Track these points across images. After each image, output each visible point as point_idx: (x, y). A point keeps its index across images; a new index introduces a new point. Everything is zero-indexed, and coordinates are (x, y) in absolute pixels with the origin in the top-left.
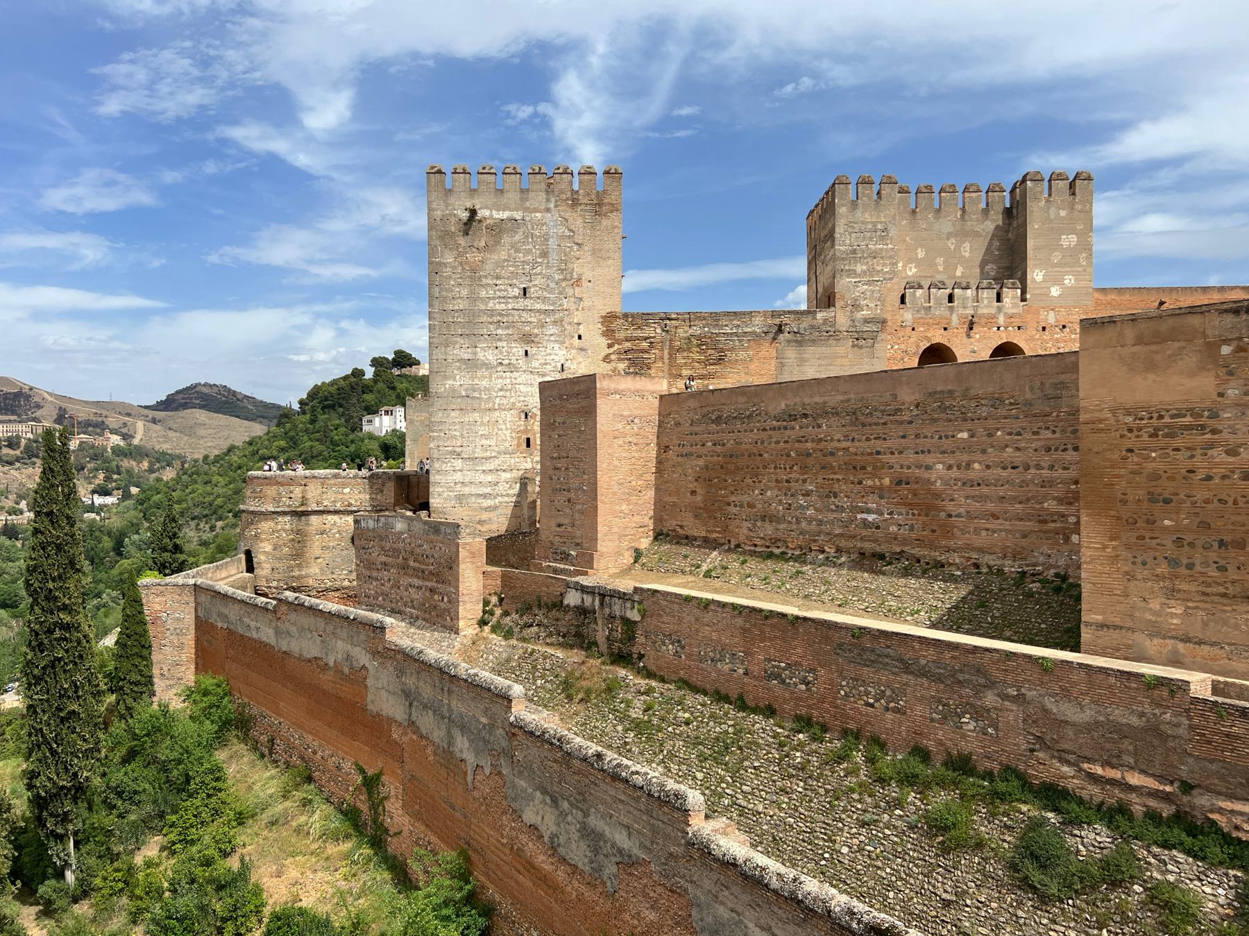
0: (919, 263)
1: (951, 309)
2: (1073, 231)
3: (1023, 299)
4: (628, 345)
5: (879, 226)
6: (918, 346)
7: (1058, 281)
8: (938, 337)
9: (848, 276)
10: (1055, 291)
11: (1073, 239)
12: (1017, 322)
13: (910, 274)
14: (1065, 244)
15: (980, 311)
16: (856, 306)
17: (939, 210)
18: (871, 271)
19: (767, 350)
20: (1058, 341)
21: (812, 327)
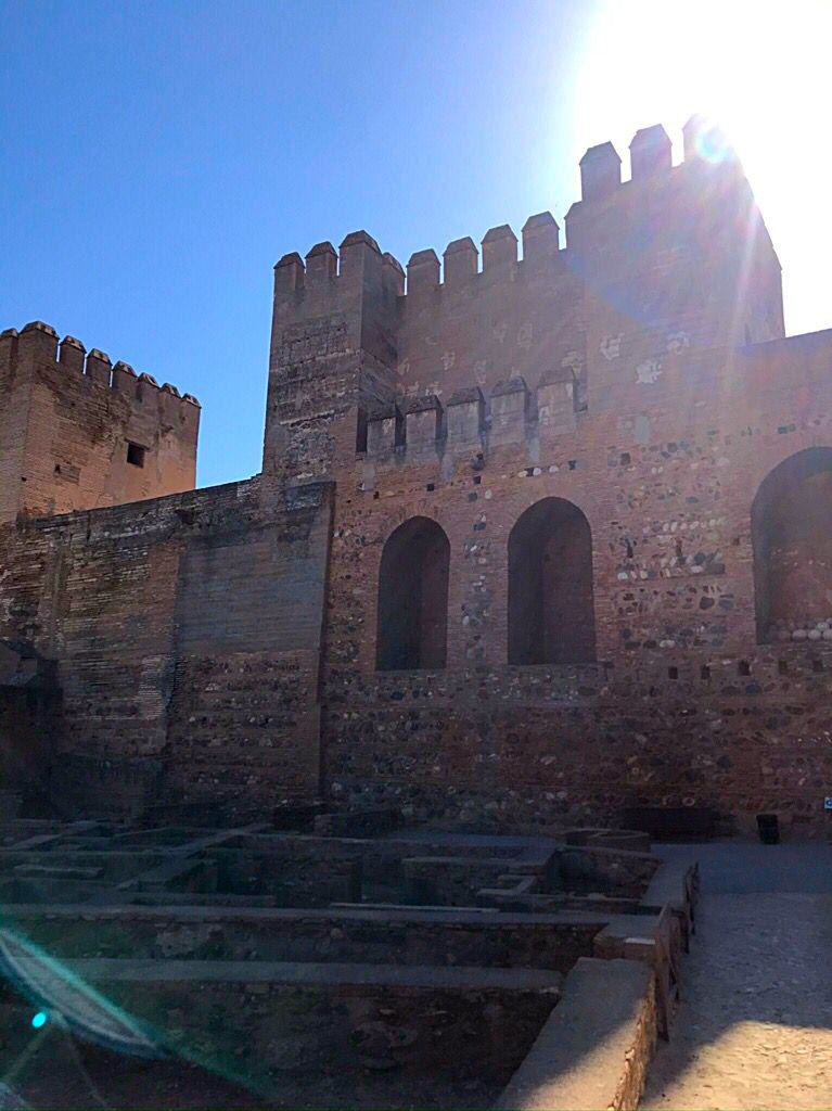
4: (17, 570)
5: (334, 323)
15: (493, 443)
18: (318, 400)
19: (170, 559)
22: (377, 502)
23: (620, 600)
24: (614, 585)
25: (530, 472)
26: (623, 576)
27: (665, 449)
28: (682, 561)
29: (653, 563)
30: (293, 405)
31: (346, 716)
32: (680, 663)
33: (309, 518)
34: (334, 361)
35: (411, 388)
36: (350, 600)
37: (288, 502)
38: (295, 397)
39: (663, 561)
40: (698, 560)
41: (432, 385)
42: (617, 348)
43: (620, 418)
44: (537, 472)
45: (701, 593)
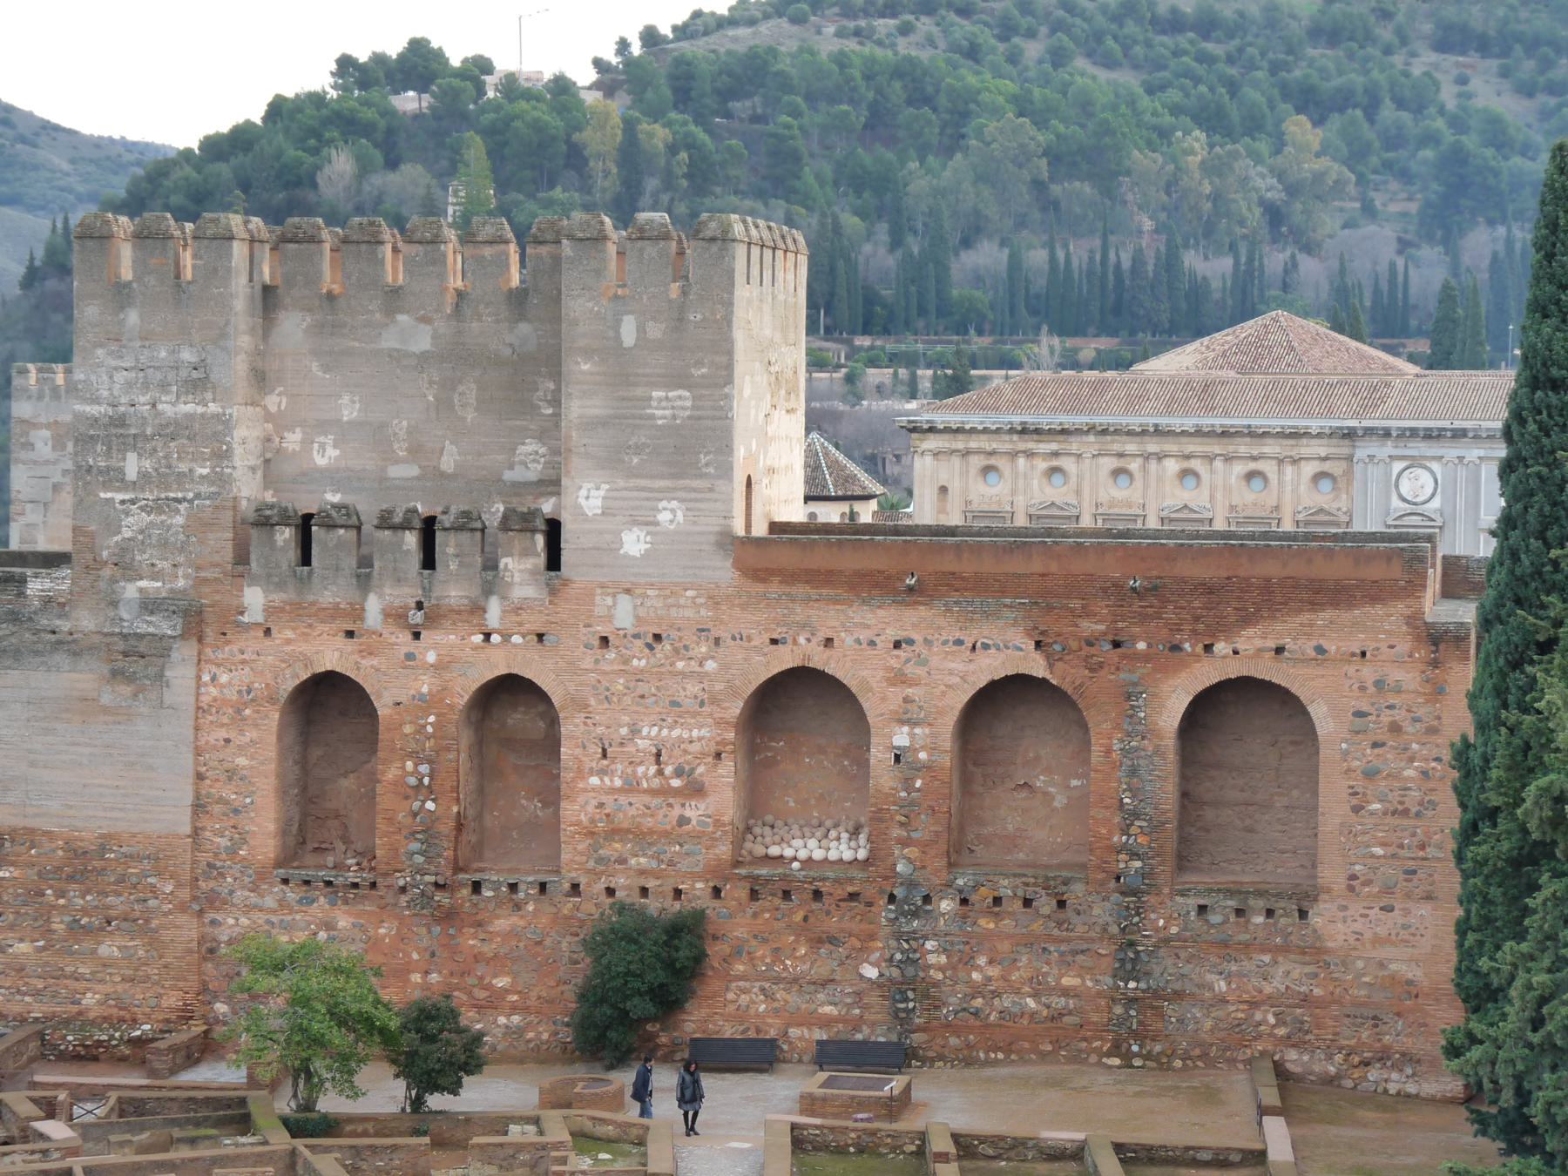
0: (343, 432)
2: (678, 380)
3: (554, 562)
8: (332, 655)
9: (106, 486)
10: (634, 543)
11: (683, 398)
12: (535, 622)
13: (321, 461)
14: (661, 414)
20: (639, 677)
22: (267, 642)
23: (590, 808)
24: (585, 790)
25: (487, 636)
26: (595, 780)
27: (650, 640)
28: (660, 773)
29: (629, 771)
30: (121, 471)
31: (231, 921)
32: (651, 884)
33: (160, 649)
34: (190, 417)
35: (289, 436)
36: (231, 774)
37: (121, 619)
38: (124, 459)
39: (641, 770)
40: (679, 773)
41: (322, 439)
42: (599, 503)
43: (599, 591)
44: (495, 638)
45: (677, 811)
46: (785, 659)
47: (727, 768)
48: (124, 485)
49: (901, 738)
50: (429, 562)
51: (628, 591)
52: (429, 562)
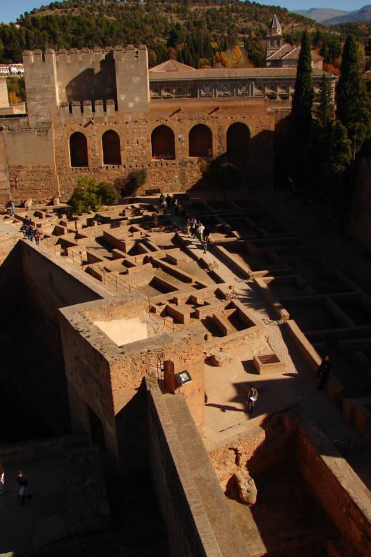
1: (82, 115)
3: (116, 109)
6: (68, 134)
7: (133, 101)
9: (33, 101)
10: (131, 105)
14: (135, 81)
15: (96, 116)
16: (37, 116)
17: (81, 62)
20: (133, 129)
21: (18, 126)
46: (159, 124)
47: (150, 145)
48: (37, 101)
49: (180, 136)
50: (93, 110)
51: (130, 113)
52: (93, 110)
